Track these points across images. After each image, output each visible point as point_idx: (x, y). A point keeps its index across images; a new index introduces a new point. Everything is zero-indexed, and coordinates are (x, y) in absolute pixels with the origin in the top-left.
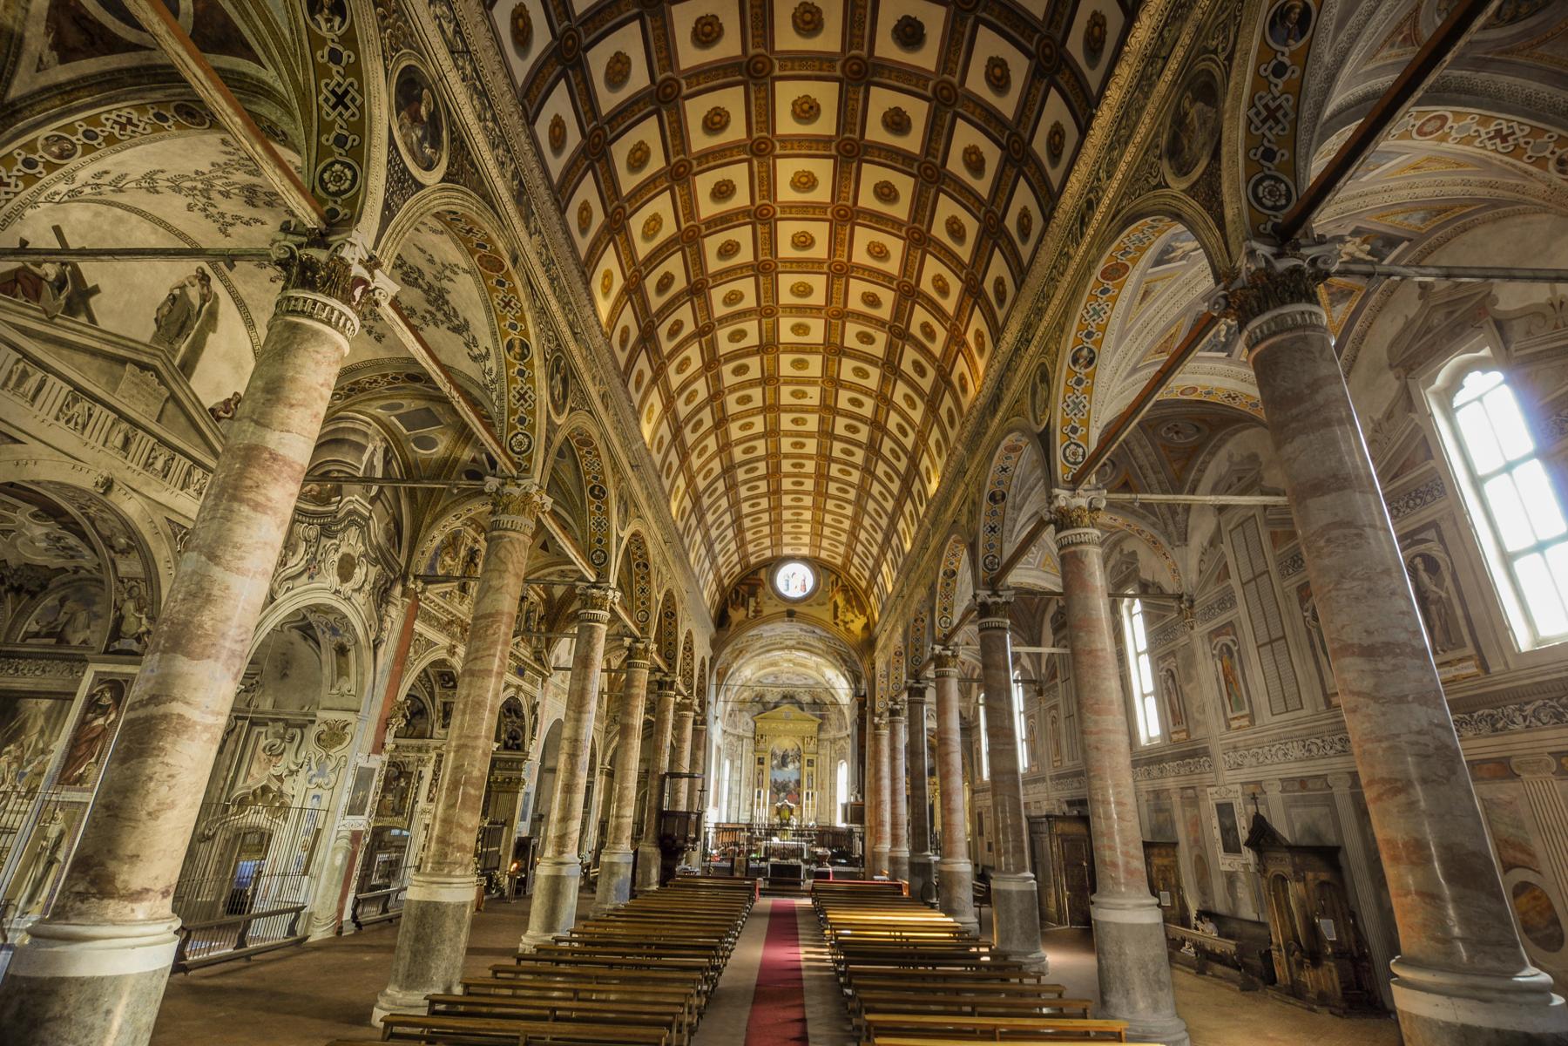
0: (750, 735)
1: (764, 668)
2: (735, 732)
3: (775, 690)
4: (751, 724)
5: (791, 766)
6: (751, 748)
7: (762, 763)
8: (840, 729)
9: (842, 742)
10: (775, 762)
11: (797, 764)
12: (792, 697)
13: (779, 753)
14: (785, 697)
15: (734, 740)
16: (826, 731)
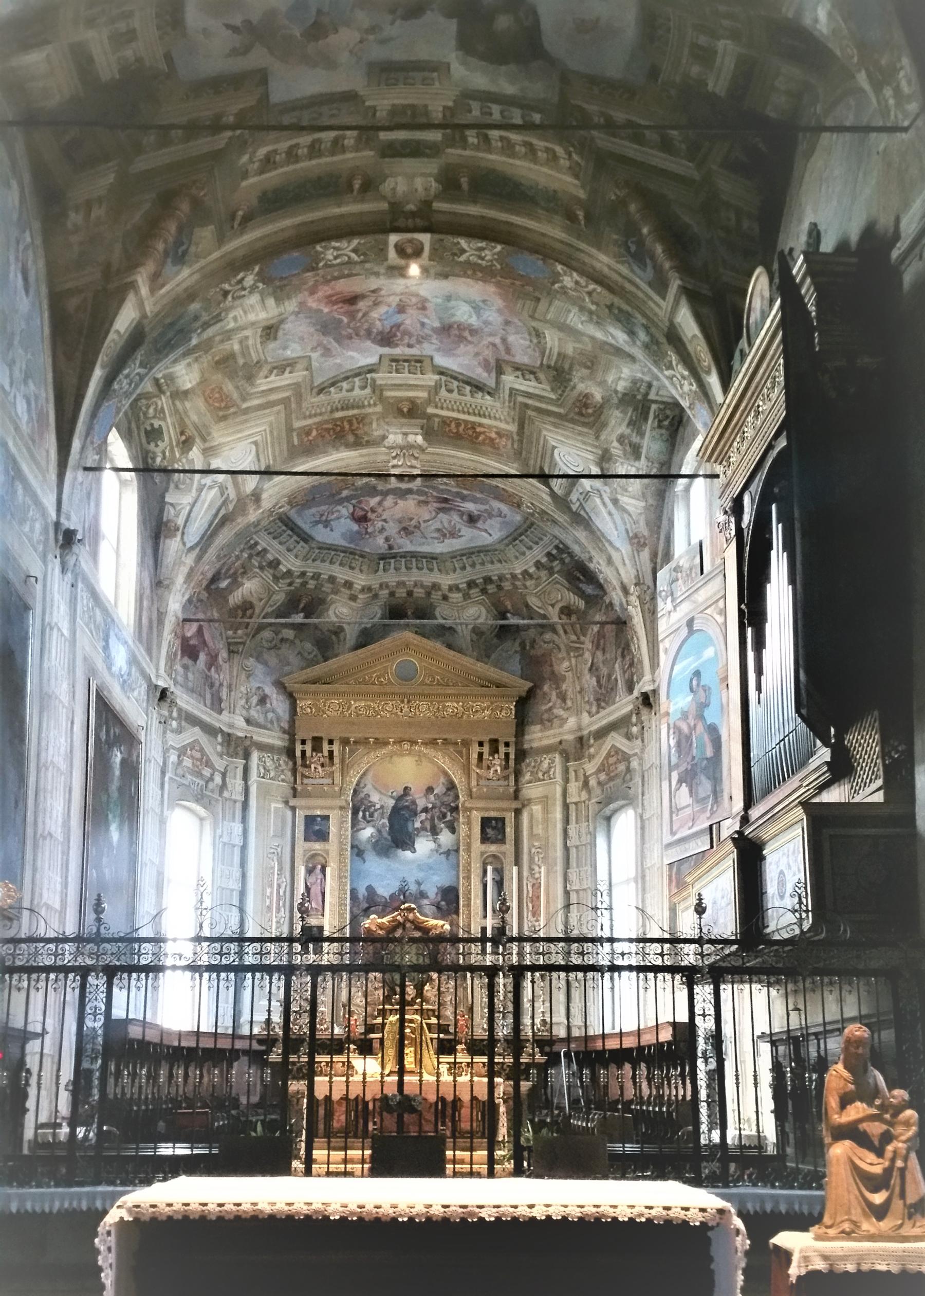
0: (275, 739)
1: (309, 450)
2: (221, 721)
3: (360, 580)
4: (278, 704)
5: (424, 846)
6: (281, 786)
7: (323, 836)
8: (604, 698)
9: (616, 740)
10: (367, 833)
11: (445, 838)
12: (424, 612)
13: (381, 800)
14: (396, 612)
15: (212, 748)
16: (547, 722)
